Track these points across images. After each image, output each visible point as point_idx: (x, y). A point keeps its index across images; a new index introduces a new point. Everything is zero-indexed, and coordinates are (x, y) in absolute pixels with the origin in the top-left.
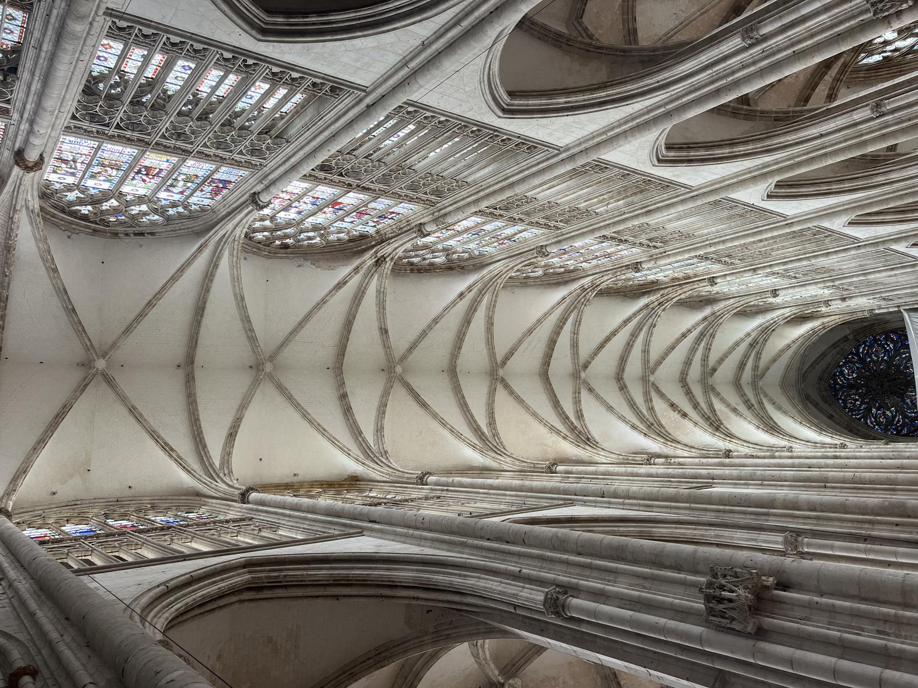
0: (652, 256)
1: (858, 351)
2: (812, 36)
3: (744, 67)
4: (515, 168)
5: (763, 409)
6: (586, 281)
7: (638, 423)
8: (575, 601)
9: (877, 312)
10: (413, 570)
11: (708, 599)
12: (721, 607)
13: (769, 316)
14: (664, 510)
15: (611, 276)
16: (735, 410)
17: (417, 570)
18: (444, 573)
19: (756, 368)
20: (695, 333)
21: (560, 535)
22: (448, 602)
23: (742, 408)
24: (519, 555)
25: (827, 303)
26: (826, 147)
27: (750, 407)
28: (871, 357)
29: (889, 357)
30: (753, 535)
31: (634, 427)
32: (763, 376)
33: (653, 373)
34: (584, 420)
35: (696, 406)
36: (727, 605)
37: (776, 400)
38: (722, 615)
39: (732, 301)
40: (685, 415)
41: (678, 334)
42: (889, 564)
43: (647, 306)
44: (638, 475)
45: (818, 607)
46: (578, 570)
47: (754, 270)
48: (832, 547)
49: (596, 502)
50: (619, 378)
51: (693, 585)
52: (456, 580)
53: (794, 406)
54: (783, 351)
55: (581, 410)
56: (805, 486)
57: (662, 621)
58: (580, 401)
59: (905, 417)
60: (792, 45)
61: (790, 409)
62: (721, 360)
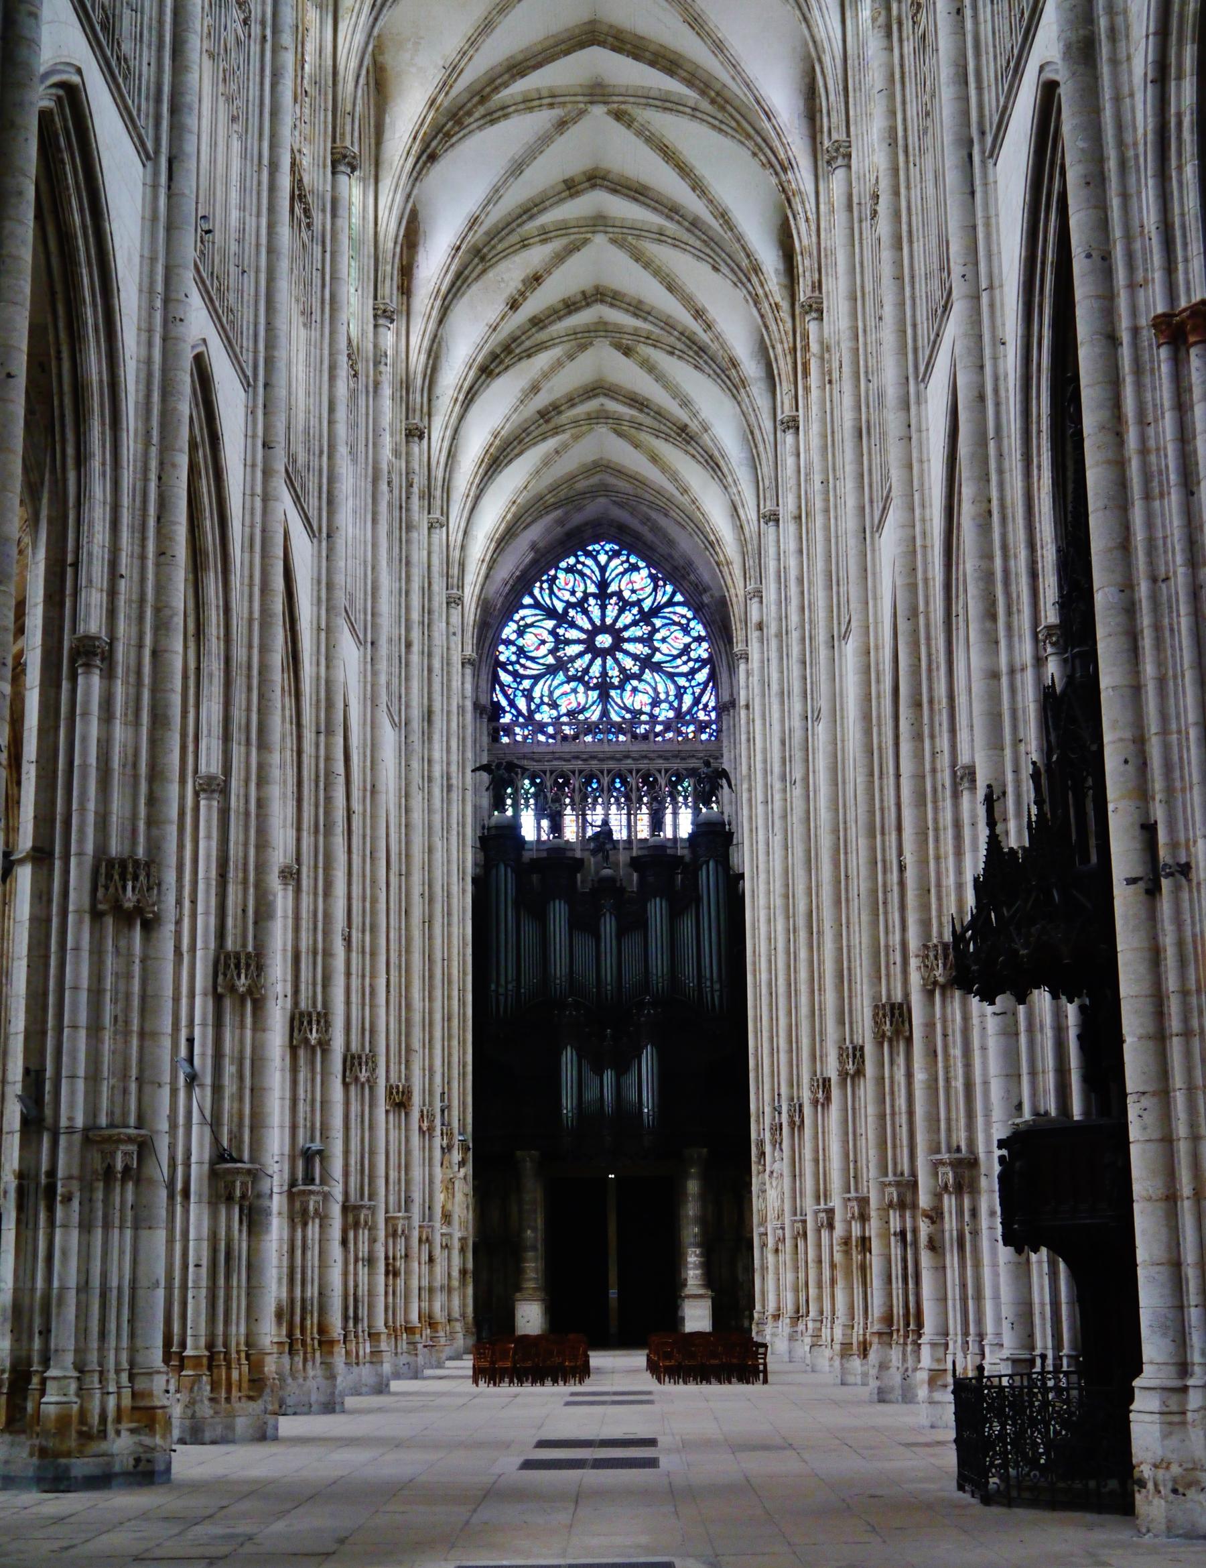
0: (828, 350)
1: (678, 604)
2: (938, 858)
3: (934, 754)
4: (920, 270)
5: (544, 437)
6: (803, 177)
7: (488, 223)
8: (96, 679)
9: (742, 667)
10: (100, 373)
11: (123, 863)
12: (116, 877)
13: (743, 475)
14: (246, 573)
15: (805, 242)
16: (535, 389)
17: (101, 381)
18: (103, 433)
19: (639, 426)
20: (704, 337)
21: (176, 619)
22: (62, 416)
23: (541, 400)
24: (143, 557)
25: (758, 594)
26: (881, 778)
27: (544, 415)
28: (664, 625)
29: (659, 664)
30: (217, 730)
31: (474, 222)
32: (620, 434)
33: (613, 241)
34: (480, 128)
35: (537, 322)
36: (119, 885)
37: (565, 456)
38: (109, 877)
39: (768, 425)
40: (514, 305)
41: (703, 299)
42: (194, 902)
43: (757, 269)
44: (332, 378)
45: (130, 963)
46: (133, 663)
47: (800, 517)
48: (208, 837)
49: (254, 436)
50: (596, 179)
51: (134, 843)
52: (96, 464)
53: (554, 488)
54: (674, 477)
55: (506, 116)
56: (318, 701)
57: (91, 806)
58: (531, 109)
59: (536, 679)
60: (936, 829)
61: (549, 478)
62: (649, 367)
